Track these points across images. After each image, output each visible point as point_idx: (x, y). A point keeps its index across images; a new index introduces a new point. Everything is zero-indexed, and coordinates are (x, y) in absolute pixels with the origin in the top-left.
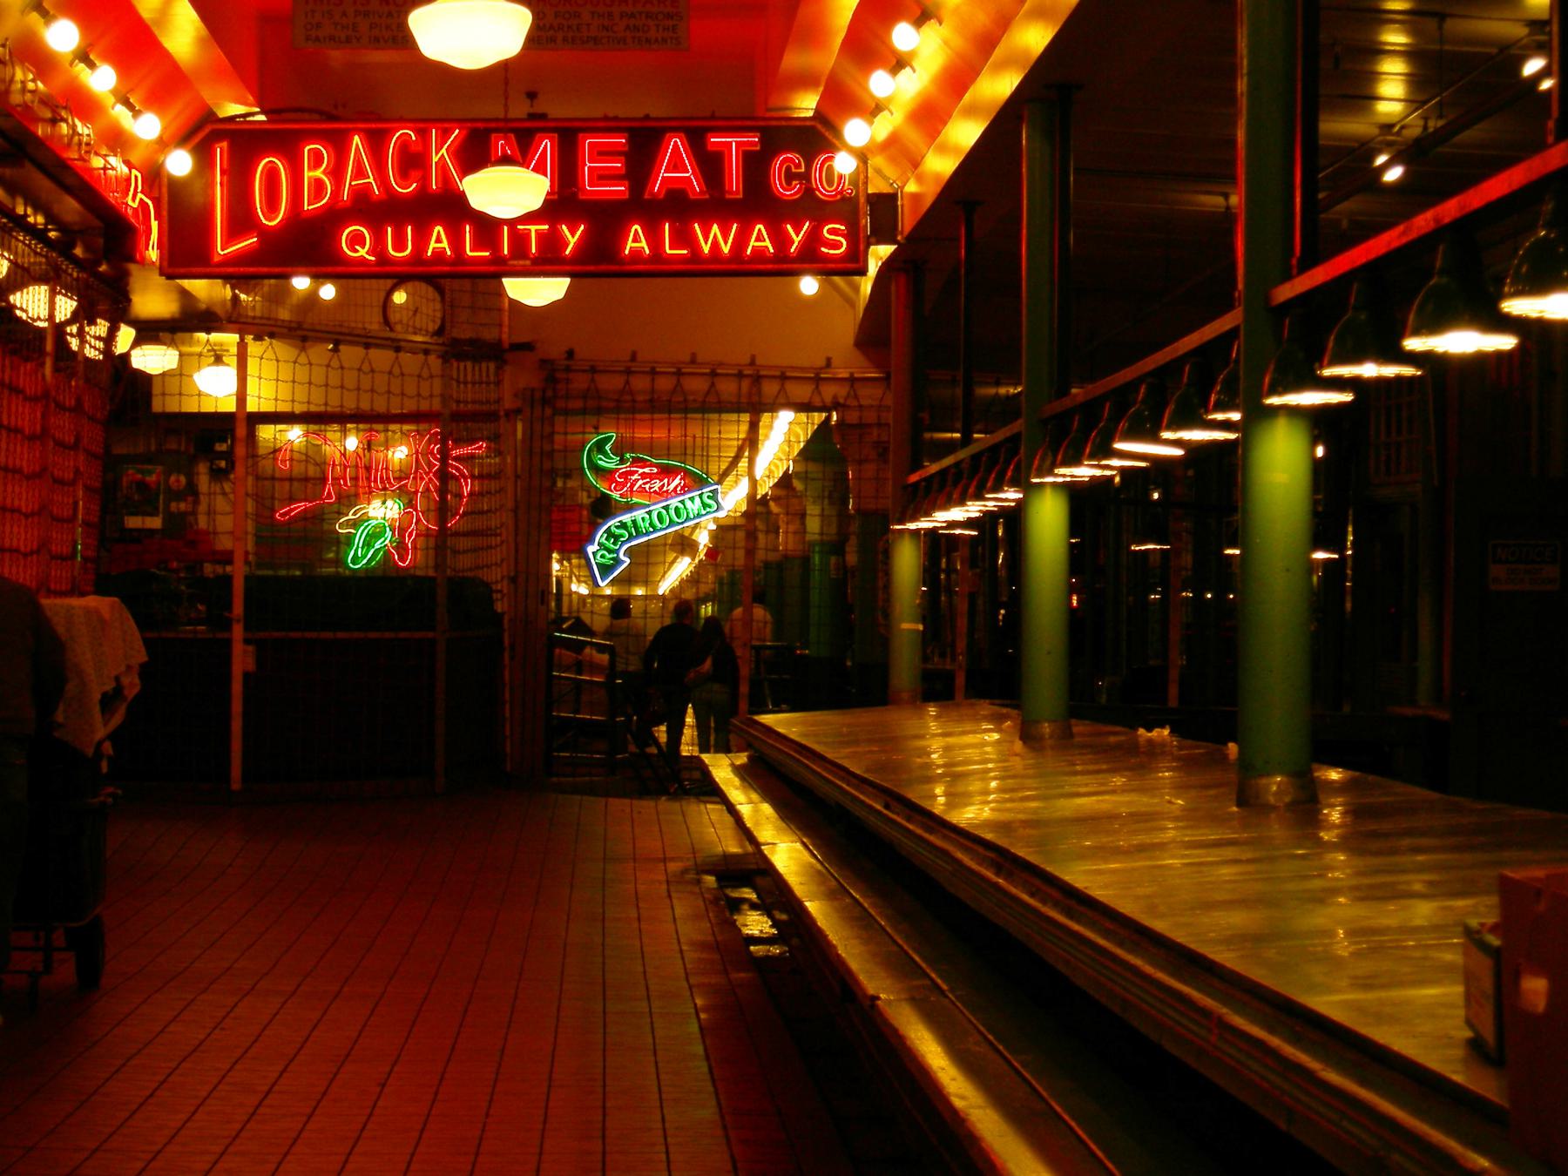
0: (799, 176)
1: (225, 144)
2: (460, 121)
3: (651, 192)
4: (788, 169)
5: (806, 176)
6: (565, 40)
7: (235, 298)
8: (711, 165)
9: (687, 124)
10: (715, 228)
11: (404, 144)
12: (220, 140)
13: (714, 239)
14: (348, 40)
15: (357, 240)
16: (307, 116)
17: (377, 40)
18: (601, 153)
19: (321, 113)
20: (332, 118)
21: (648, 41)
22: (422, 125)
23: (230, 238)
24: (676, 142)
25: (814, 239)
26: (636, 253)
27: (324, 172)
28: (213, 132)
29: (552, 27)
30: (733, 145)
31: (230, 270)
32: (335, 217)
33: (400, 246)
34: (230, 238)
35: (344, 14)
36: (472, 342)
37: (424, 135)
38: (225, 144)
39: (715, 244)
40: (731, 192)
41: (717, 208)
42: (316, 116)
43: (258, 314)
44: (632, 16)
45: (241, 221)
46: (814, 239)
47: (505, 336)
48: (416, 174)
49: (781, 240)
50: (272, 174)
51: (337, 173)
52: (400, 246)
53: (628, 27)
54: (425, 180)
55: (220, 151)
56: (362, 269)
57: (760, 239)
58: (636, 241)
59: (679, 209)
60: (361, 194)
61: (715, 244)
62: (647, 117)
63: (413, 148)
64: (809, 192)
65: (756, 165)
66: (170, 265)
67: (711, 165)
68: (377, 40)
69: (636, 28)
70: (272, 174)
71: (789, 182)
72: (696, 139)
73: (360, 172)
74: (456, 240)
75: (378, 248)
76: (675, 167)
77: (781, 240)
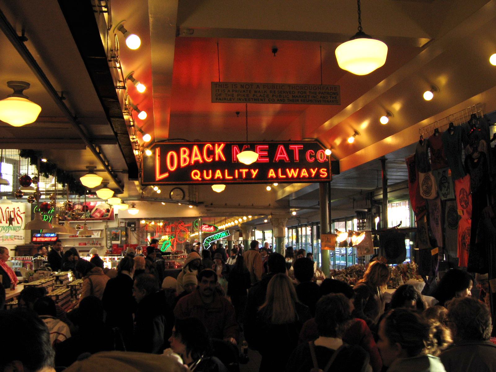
0: (313, 156)
1: (159, 148)
2: (223, 142)
3: (275, 161)
4: (310, 154)
5: (315, 157)
6: (301, 101)
7: (142, 192)
8: (290, 153)
9: (284, 142)
10: (292, 170)
11: (208, 149)
12: (157, 147)
13: (292, 173)
14: (230, 100)
15: (196, 174)
16: (180, 141)
17: (240, 99)
18: (261, 150)
19: (184, 140)
20: (188, 141)
21: (328, 101)
22: (213, 143)
23: (161, 173)
24: (282, 147)
25: (318, 173)
26: (272, 177)
27: (187, 156)
28: (155, 145)
29: (297, 96)
30: (296, 148)
31: (160, 183)
32: (190, 168)
33: (208, 175)
34: (161, 173)
35: (229, 91)
36: (449, 199)
37: (214, 146)
38: (159, 148)
39: (293, 175)
40: (296, 160)
41: (292, 165)
42: (183, 141)
43: (146, 196)
44: (322, 93)
45: (164, 169)
46: (318, 173)
47: (197, 201)
48: (212, 156)
49: (310, 173)
50: (172, 157)
51: (190, 156)
52: (208, 175)
53: (321, 97)
54: (214, 158)
55: (158, 150)
56: (197, 182)
57: (304, 173)
58: (272, 173)
59: (283, 165)
60: (197, 162)
61: (293, 175)
62: (272, 141)
63: (211, 149)
64: (316, 160)
65: (302, 153)
66: (144, 181)
67: (290, 153)
68: (240, 99)
69: (324, 97)
70: (172, 157)
71: (310, 158)
72: (286, 146)
73: (196, 156)
74: (223, 174)
75: (202, 176)
76: (281, 154)
77: (310, 173)
